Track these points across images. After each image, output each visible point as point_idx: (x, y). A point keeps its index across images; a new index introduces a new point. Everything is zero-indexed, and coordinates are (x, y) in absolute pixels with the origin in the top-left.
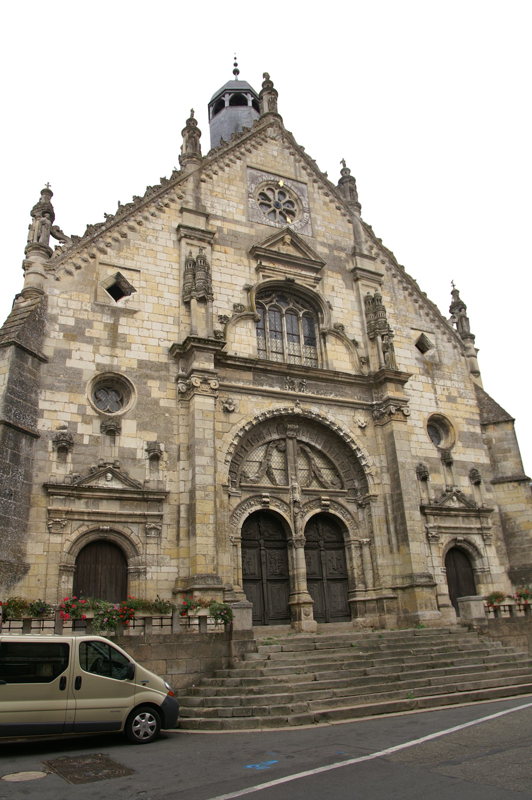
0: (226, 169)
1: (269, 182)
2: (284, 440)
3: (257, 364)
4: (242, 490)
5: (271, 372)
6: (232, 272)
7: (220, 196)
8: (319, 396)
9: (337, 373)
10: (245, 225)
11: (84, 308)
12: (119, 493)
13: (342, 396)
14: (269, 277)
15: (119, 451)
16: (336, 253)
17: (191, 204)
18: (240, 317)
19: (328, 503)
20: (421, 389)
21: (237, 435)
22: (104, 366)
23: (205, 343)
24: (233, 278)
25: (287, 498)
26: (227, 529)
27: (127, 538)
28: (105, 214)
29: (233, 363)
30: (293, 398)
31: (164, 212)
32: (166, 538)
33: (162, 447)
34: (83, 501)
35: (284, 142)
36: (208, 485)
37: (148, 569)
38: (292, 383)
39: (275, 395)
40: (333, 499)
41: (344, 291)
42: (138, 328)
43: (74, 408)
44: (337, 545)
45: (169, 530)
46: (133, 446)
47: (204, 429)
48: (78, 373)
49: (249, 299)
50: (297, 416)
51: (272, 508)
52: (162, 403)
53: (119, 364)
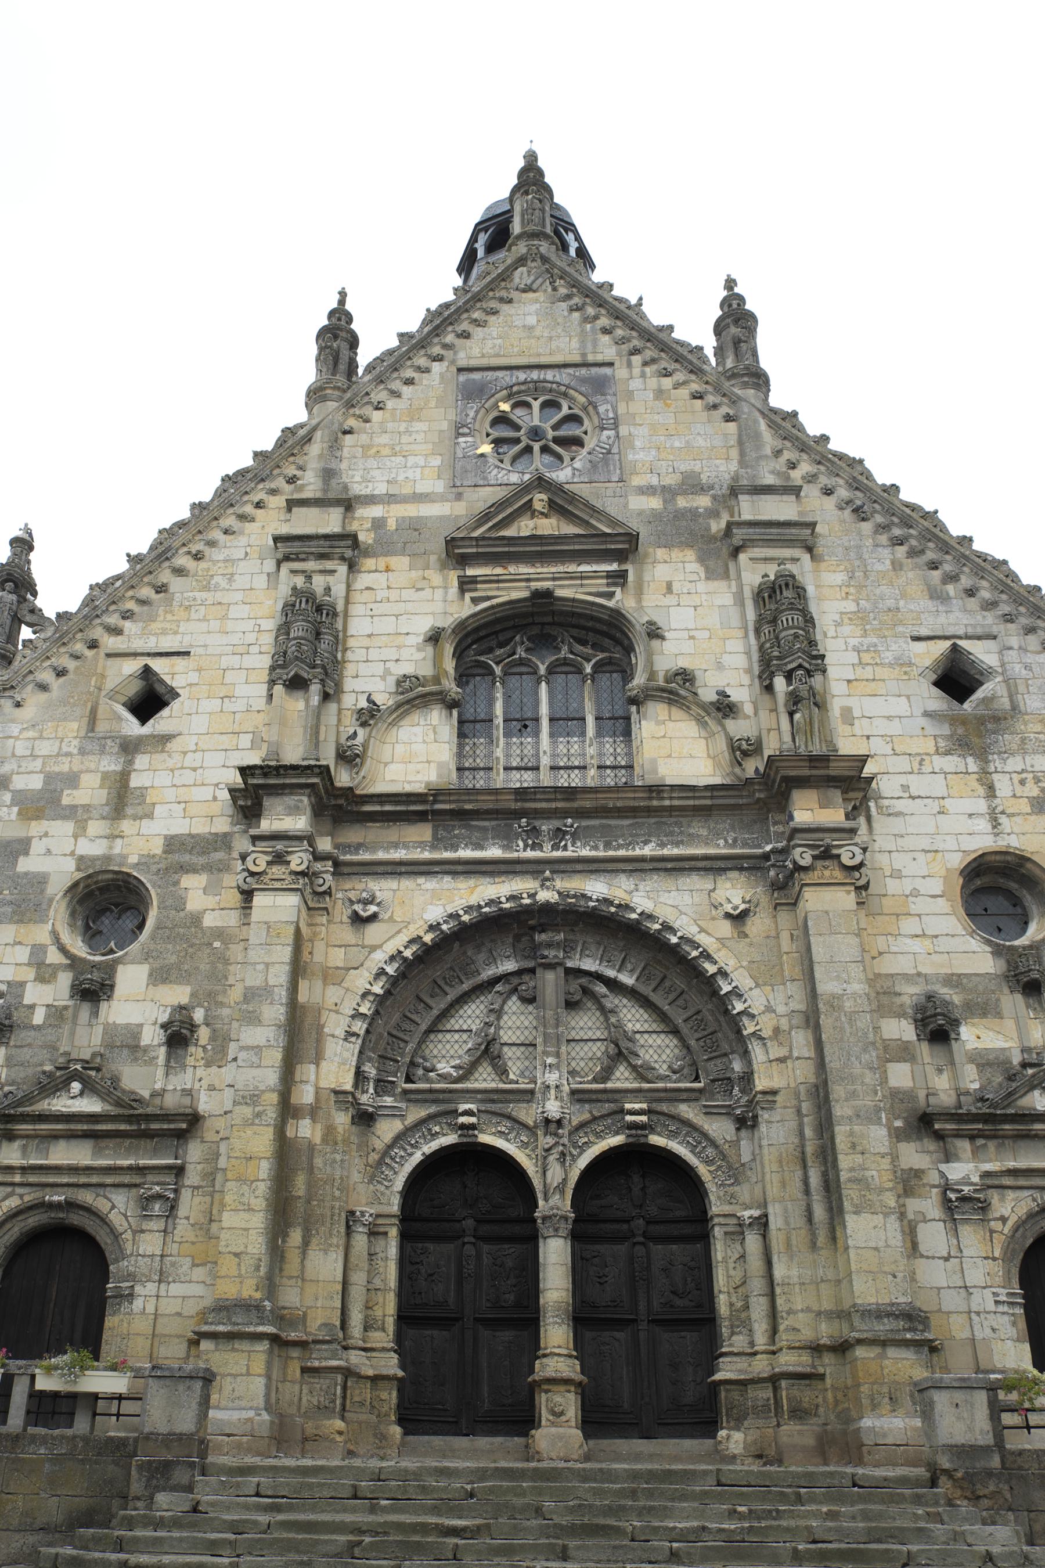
0: (406, 390)
1: (515, 389)
2: (532, 971)
3: (435, 802)
4: (409, 1101)
5: (476, 814)
6: (400, 608)
7: (386, 451)
8: (611, 853)
9: (656, 790)
10: (441, 498)
11: (65, 749)
12: (88, 1122)
13: (677, 844)
14: (489, 598)
15: (105, 1032)
16: (682, 502)
17: (311, 487)
18: (408, 702)
19: (644, 1118)
20: (942, 791)
21: (382, 972)
22: (94, 859)
23: (278, 775)
24: (399, 619)
25: (528, 1114)
26: (337, 1193)
27: (103, 1220)
28: (128, 555)
29: (378, 808)
30: (534, 867)
31: (253, 520)
32: (187, 1218)
33: (198, 1015)
34: (17, 1144)
35: (555, 289)
36: (263, 1092)
37: (138, 1289)
38: (535, 831)
39: (484, 868)
40: (664, 1107)
41: (702, 586)
42: (172, 770)
43: (23, 954)
44: (688, 1230)
45: (197, 1200)
46: (135, 1020)
47: (267, 965)
48: (41, 880)
49: (437, 660)
50: (547, 908)
51: (485, 1138)
52: (209, 921)
53: (125, 852)
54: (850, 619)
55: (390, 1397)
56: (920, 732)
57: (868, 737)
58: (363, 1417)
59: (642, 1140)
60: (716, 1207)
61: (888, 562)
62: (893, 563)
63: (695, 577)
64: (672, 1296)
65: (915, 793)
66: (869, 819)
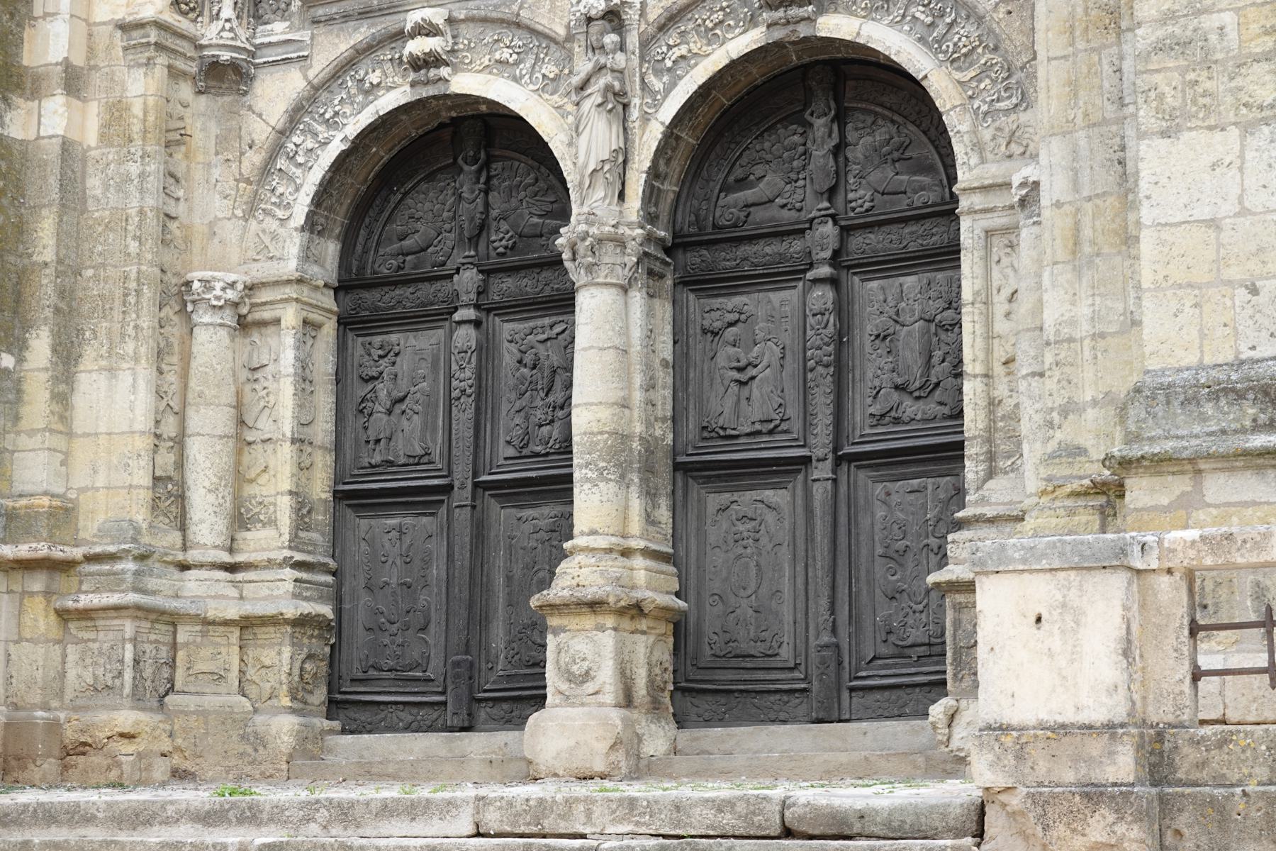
4: (316, 22)
51: (465, 83)
55: (279, 658)
58: (210, 702)
59: (803, 31)
60: (969, 171)
64: (896, 396)
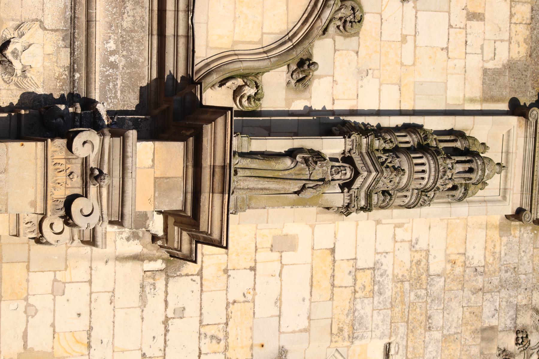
41: (475, 63)
54: (418, 263)
56: (258, 341)
57: (253, 269)
61: (494, 322)
62: (492, 328)
63: (488, 55)
65: (174, 325)
66: (137, 258)
